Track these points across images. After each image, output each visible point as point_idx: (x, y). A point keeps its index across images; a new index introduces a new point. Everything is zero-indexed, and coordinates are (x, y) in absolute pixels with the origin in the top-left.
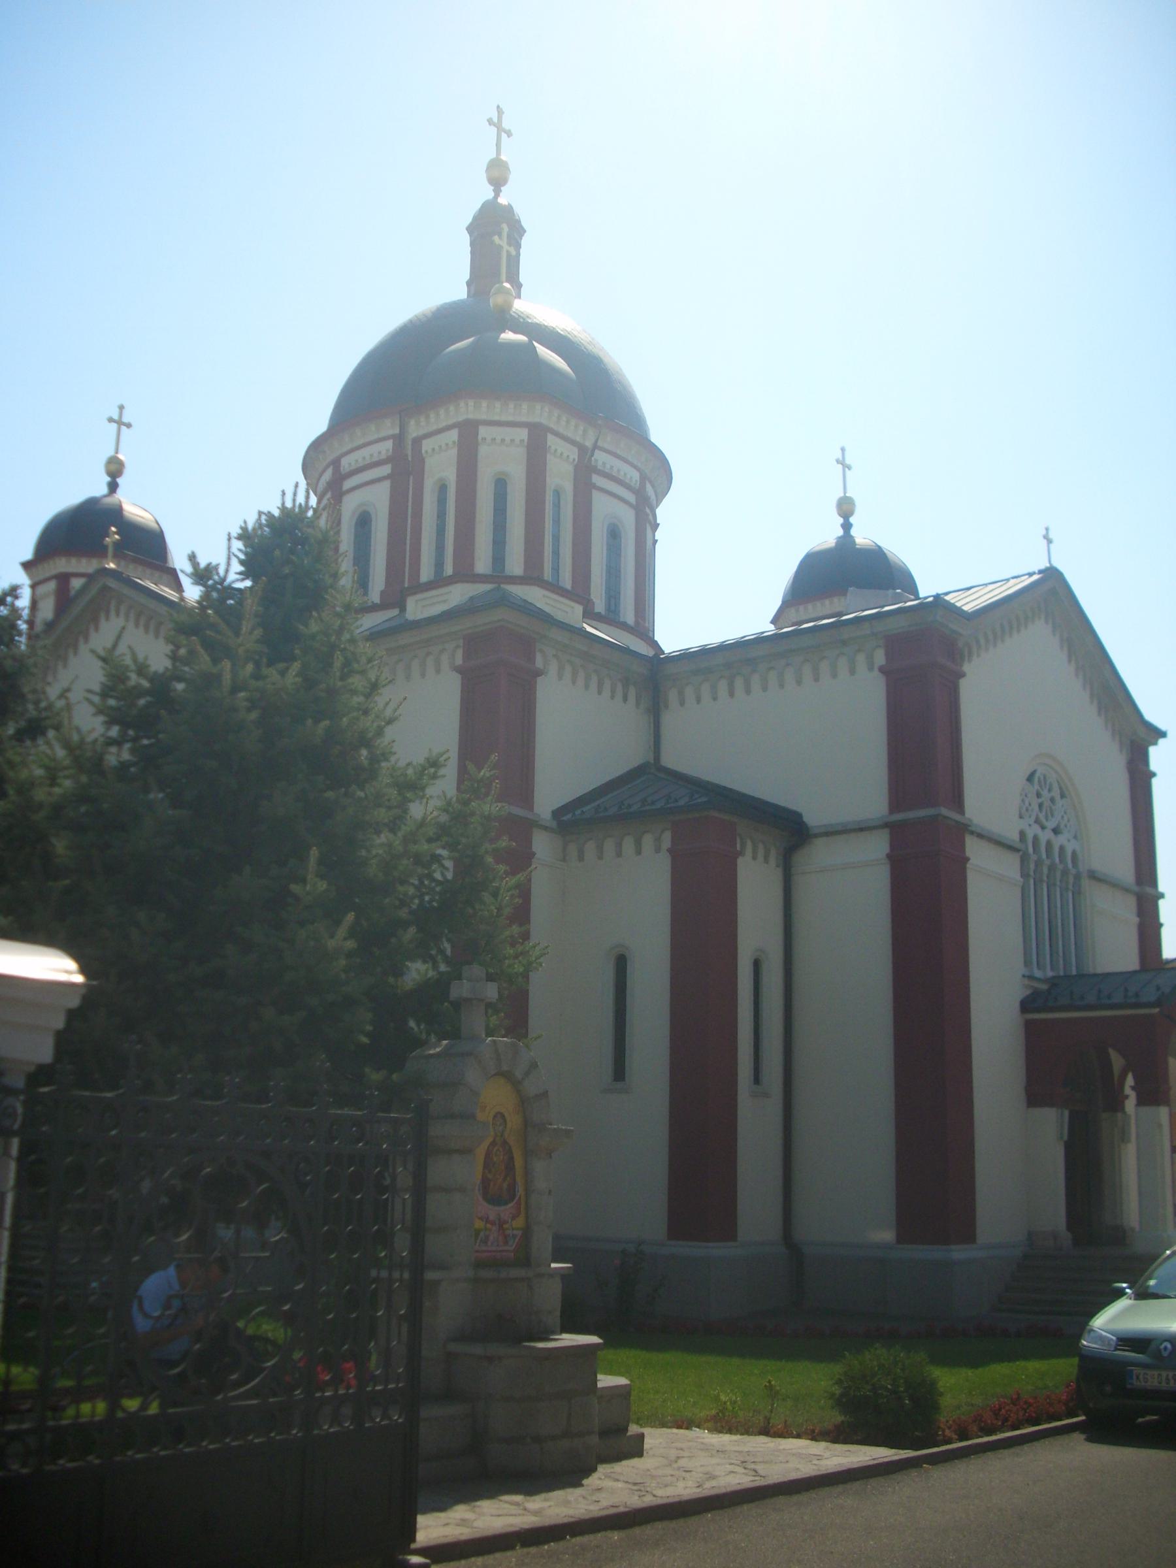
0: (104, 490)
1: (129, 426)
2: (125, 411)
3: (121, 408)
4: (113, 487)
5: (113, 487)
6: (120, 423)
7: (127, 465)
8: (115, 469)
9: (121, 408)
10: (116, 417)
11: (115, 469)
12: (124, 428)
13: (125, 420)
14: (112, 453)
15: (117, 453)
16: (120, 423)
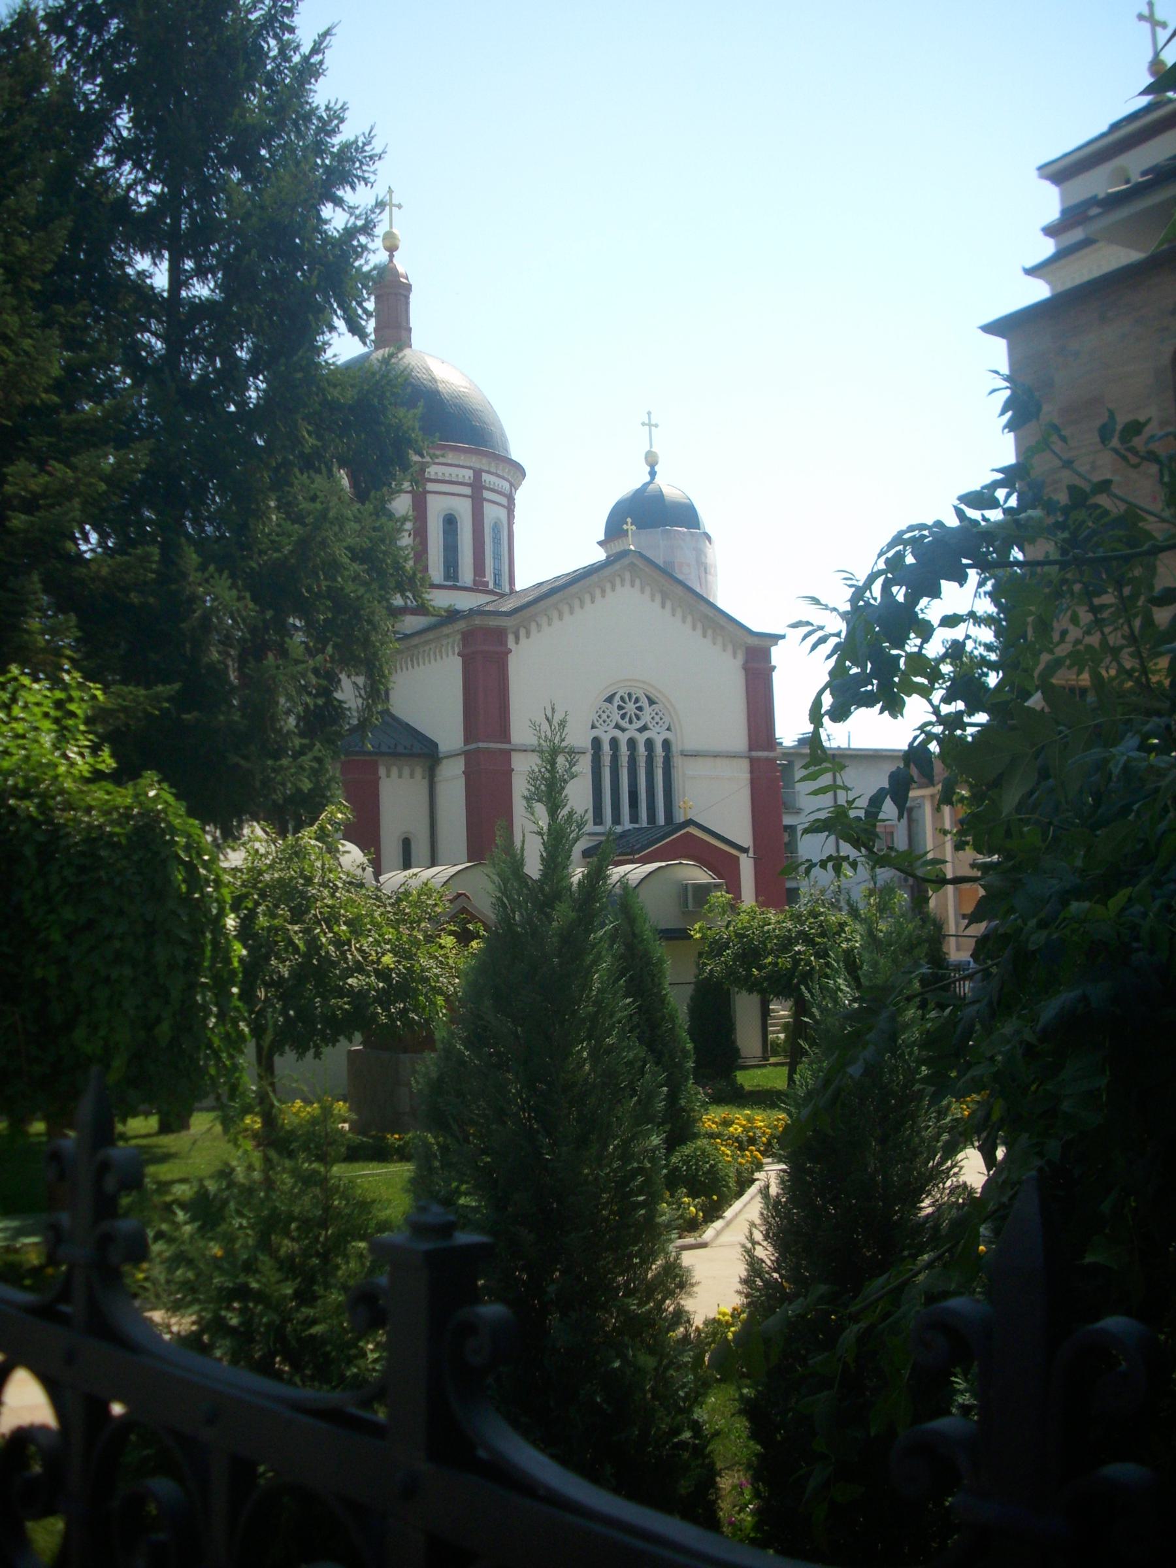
0: (648, 478)
1: (656, 426)
2: (652, 416)
3: (649, 413)
4: (653, 474)
5: (653, 474)
6: (650, 425)
7: (660, 454)
8: (652, 461)
9: (649, 413)
10: (647, 422)
11: (652, 461)
12: (653, 428)
13: (653, 422)
14: (648, 448)
15: (651, 447)
16: (650, 425)
